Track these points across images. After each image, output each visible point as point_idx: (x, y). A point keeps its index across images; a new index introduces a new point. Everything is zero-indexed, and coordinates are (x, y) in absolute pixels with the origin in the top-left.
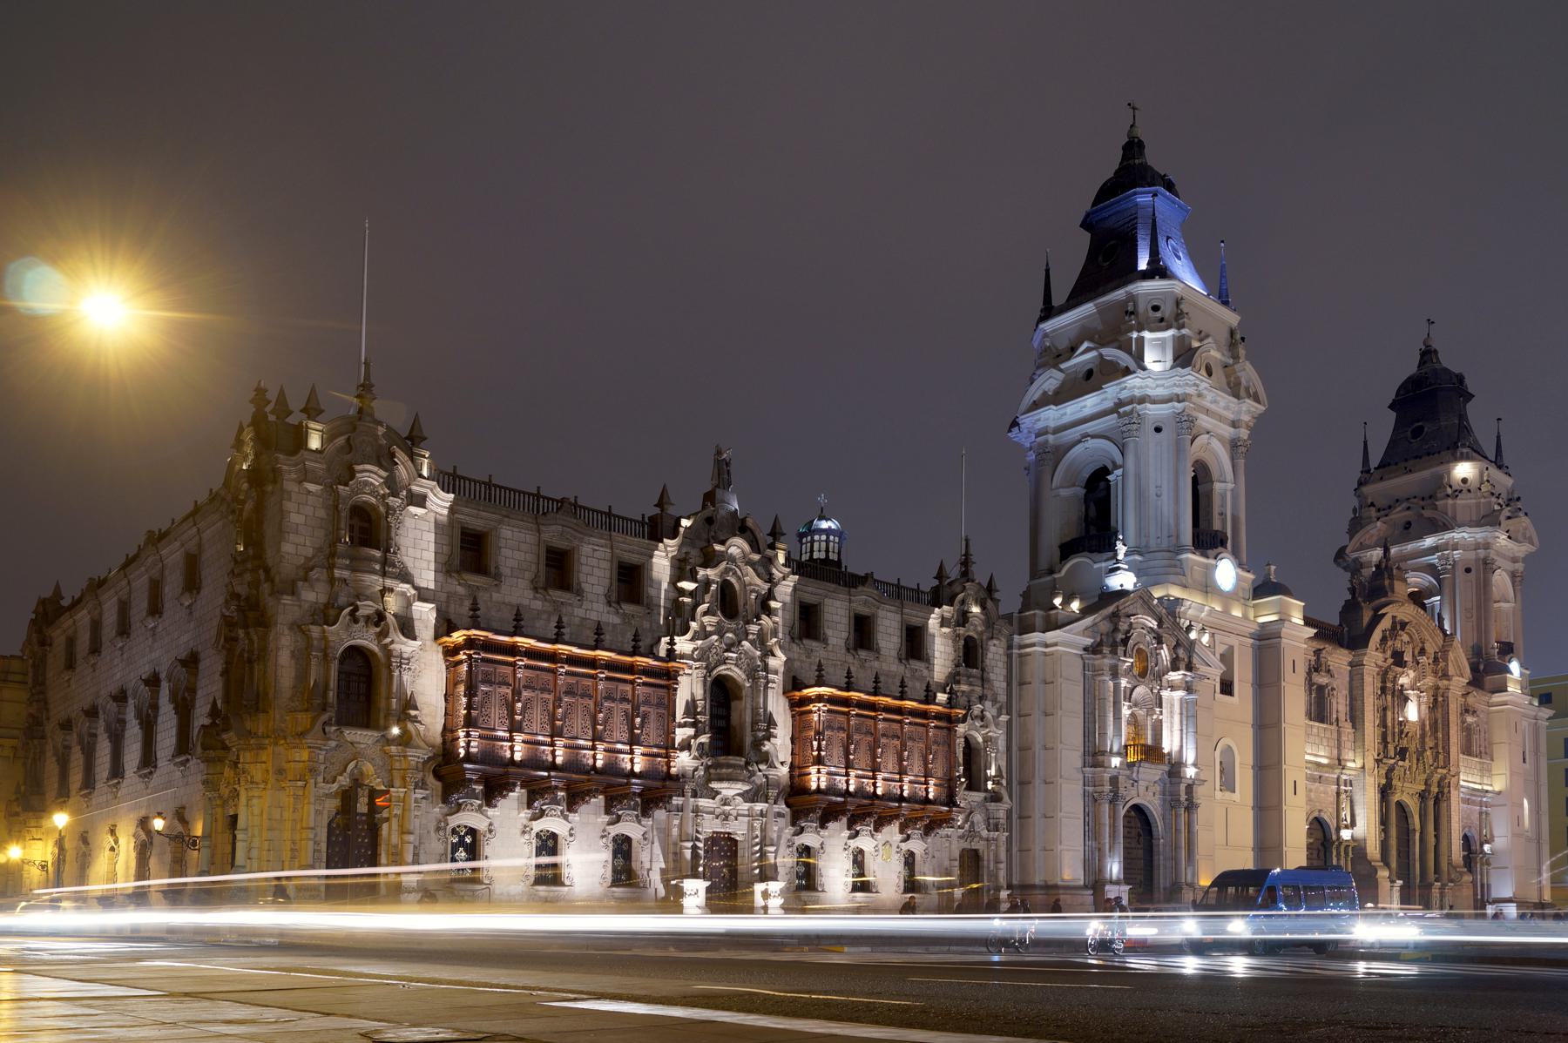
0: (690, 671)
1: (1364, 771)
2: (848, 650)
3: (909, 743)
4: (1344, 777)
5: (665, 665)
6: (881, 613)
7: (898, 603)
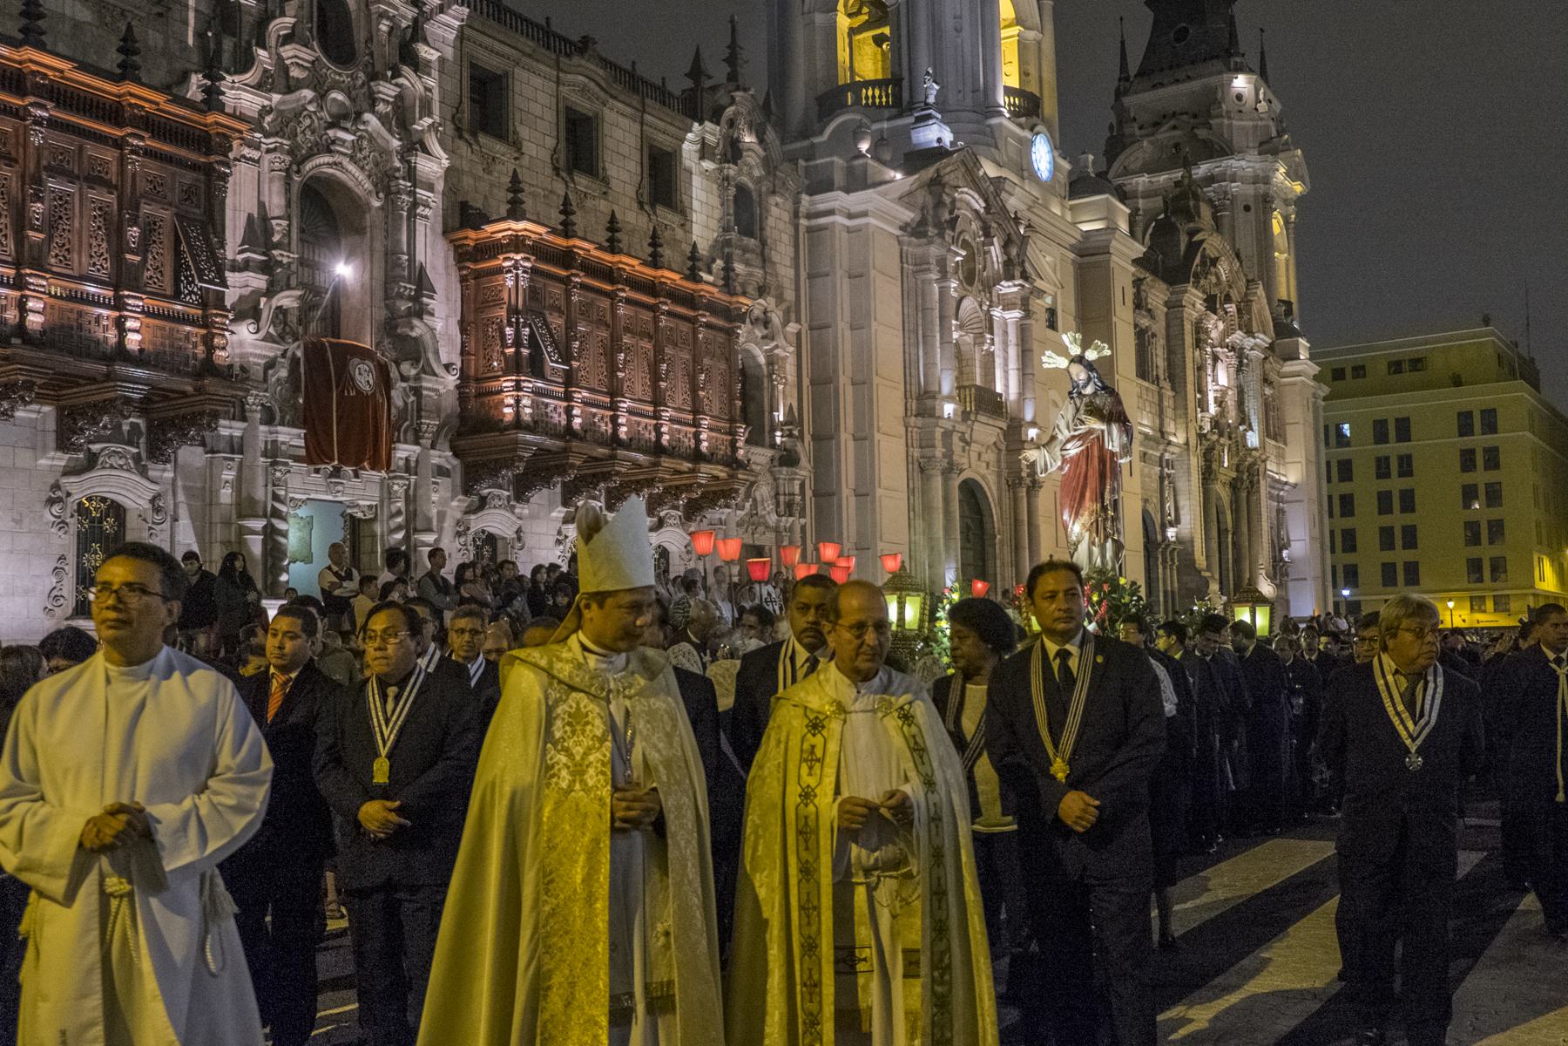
0: (255, 155)
1: (1188, 449)
2: (556, 170)
3: (668, 350)
4: (1167, 456)
5: (195, 116)
6: (609, 116)
7: (635, 100)
